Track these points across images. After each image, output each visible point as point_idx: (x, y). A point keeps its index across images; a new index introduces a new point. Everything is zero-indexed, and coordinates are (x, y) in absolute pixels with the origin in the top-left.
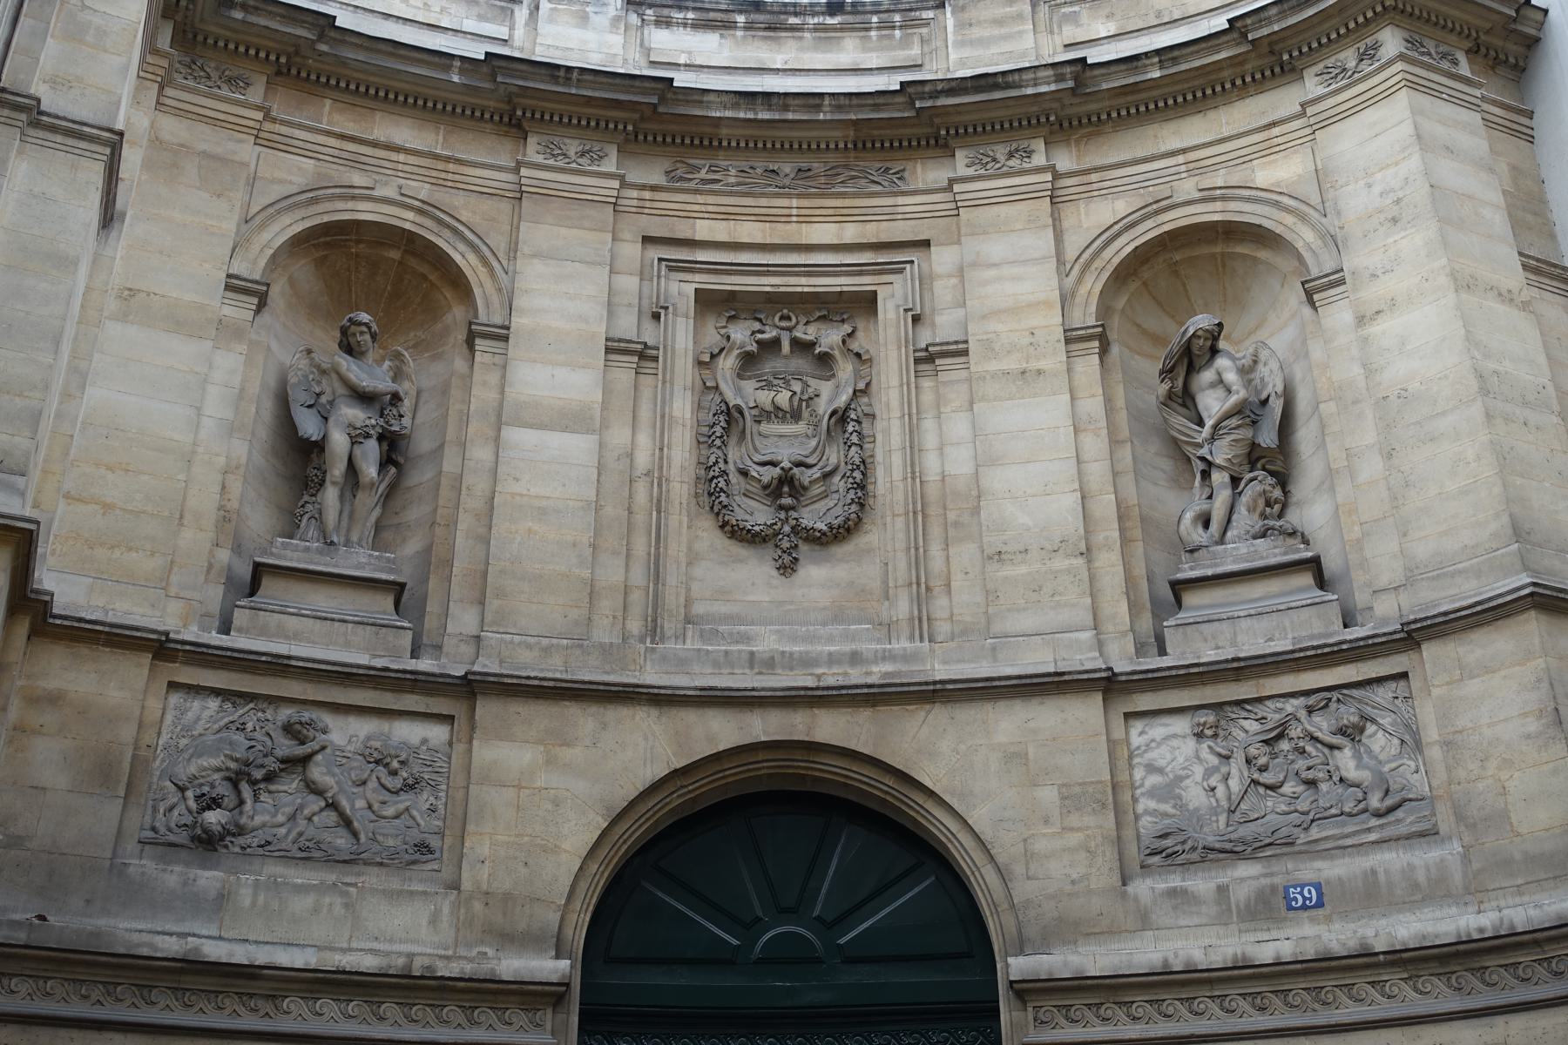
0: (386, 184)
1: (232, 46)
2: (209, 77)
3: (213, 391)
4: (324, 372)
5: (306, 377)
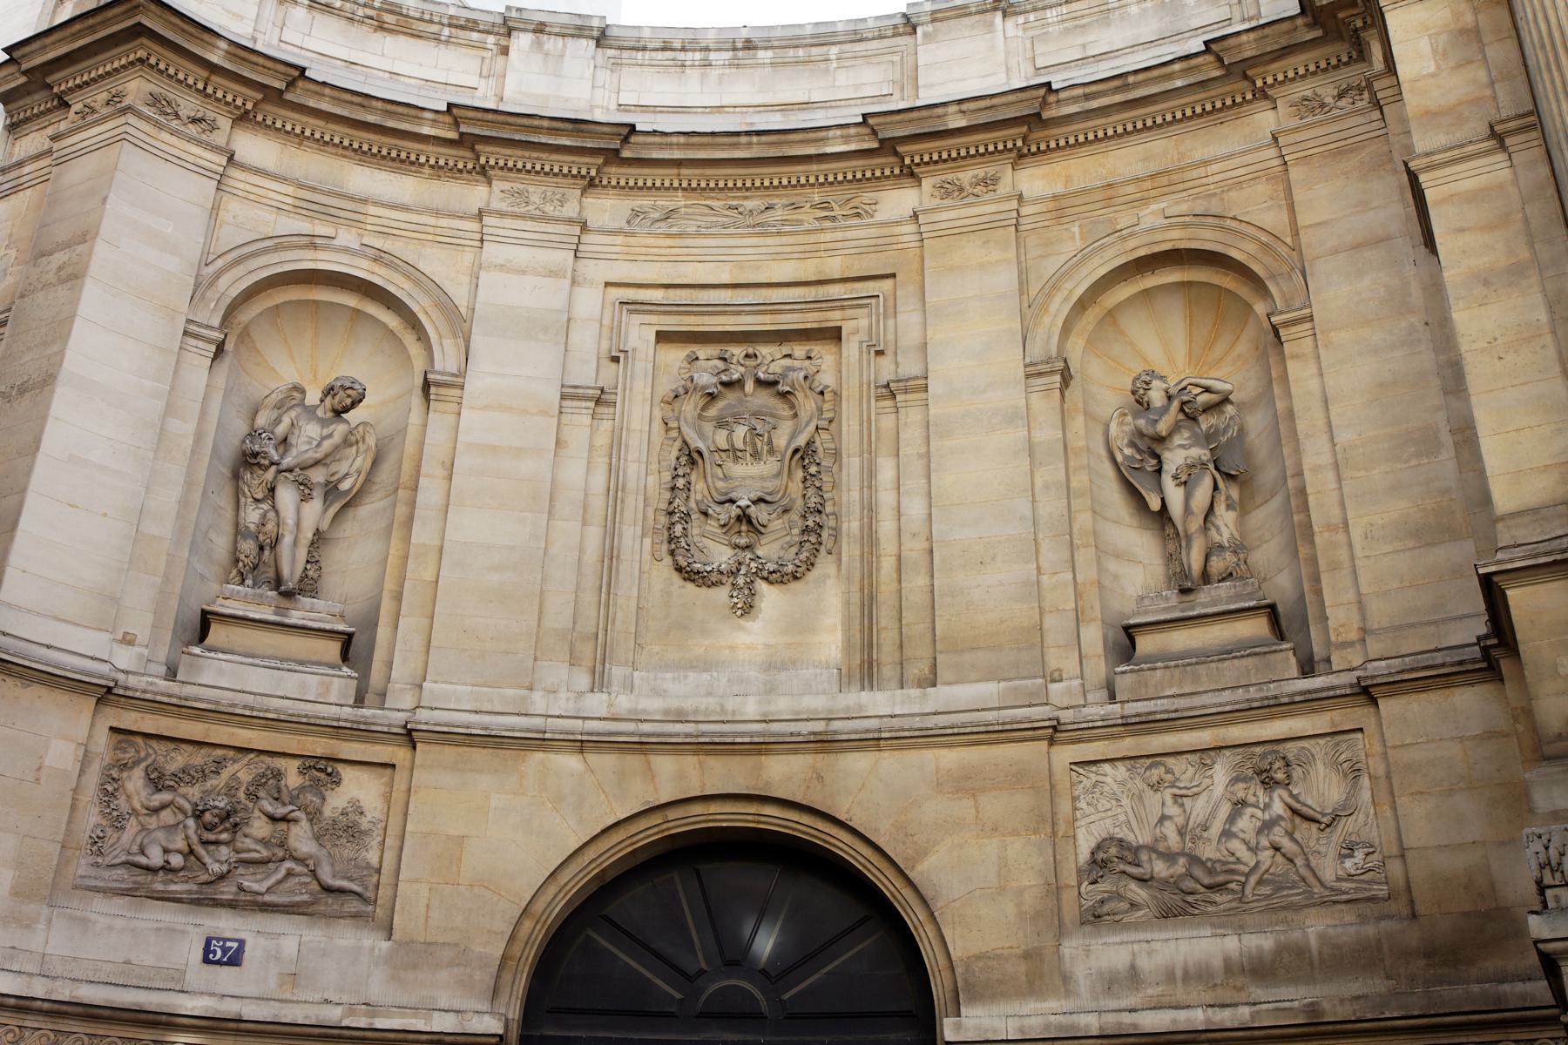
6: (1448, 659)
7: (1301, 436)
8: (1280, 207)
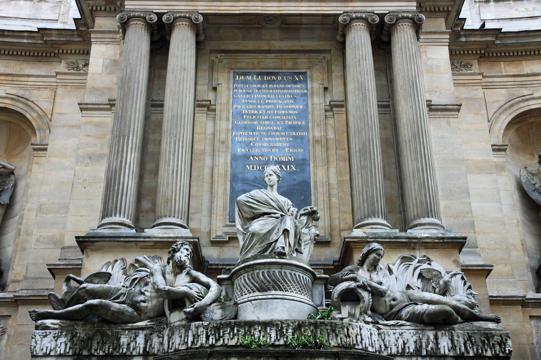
0: (537, 91)
1: (462, 52)
2: (456, 67)
3: (503, 194)
4: (534, 175)
5: (527, 178)
8: (51, 102)
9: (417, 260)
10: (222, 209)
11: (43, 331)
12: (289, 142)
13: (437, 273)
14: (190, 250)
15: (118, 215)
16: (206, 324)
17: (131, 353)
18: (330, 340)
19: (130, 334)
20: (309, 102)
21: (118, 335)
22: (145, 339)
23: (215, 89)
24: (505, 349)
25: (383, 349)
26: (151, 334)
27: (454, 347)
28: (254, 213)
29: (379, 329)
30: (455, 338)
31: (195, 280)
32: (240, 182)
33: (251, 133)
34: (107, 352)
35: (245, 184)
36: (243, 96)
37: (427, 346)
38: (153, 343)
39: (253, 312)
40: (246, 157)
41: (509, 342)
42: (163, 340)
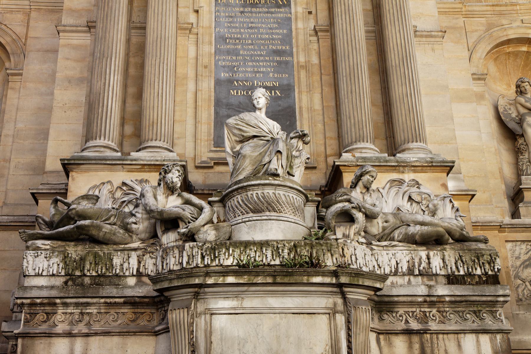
5: (504, 108)
6: (30, 220)
7: (5, 121)
8: (24, 26)
9: (406, 184)
10: (206, 134)
11: (34, 252)
12: (273, 67)
13: (427, 196)
14: (181, 172)
15: (102, 138)
16: (200, 245)
17: (124, 274)
18: (326, 260)
19: (122, 255)
20: (293, 27)
21: (110, 256)
22: (138, 260)
23: (197, 11)
24: (494, 266)
25: (376, 269)
26: (144, 255)
27: (445, 266)
28: (243, 136)
29: (372, 249)
30: (447, 258)
31: (188, 202)
32: (224, 107)
33: (234, 58)
34: (100, 272)
35: (229, 109)
36: (225, 19)
37: (419, 266)
38: (147, 264)
39: (248, 233)
40: (230, 81)
41: (498, 260)
42: (156, 261)
